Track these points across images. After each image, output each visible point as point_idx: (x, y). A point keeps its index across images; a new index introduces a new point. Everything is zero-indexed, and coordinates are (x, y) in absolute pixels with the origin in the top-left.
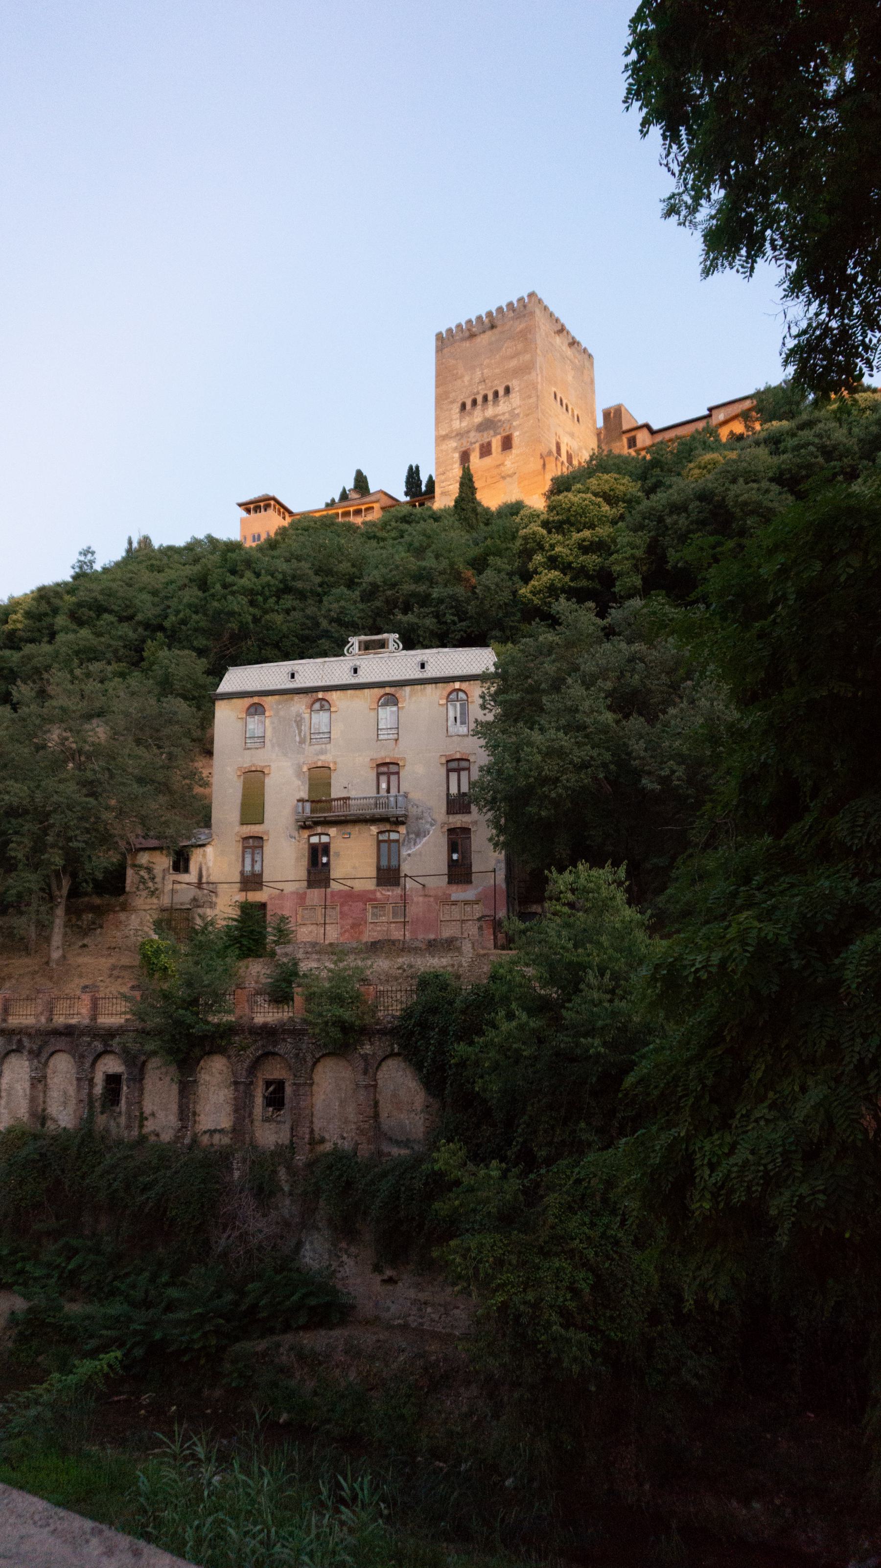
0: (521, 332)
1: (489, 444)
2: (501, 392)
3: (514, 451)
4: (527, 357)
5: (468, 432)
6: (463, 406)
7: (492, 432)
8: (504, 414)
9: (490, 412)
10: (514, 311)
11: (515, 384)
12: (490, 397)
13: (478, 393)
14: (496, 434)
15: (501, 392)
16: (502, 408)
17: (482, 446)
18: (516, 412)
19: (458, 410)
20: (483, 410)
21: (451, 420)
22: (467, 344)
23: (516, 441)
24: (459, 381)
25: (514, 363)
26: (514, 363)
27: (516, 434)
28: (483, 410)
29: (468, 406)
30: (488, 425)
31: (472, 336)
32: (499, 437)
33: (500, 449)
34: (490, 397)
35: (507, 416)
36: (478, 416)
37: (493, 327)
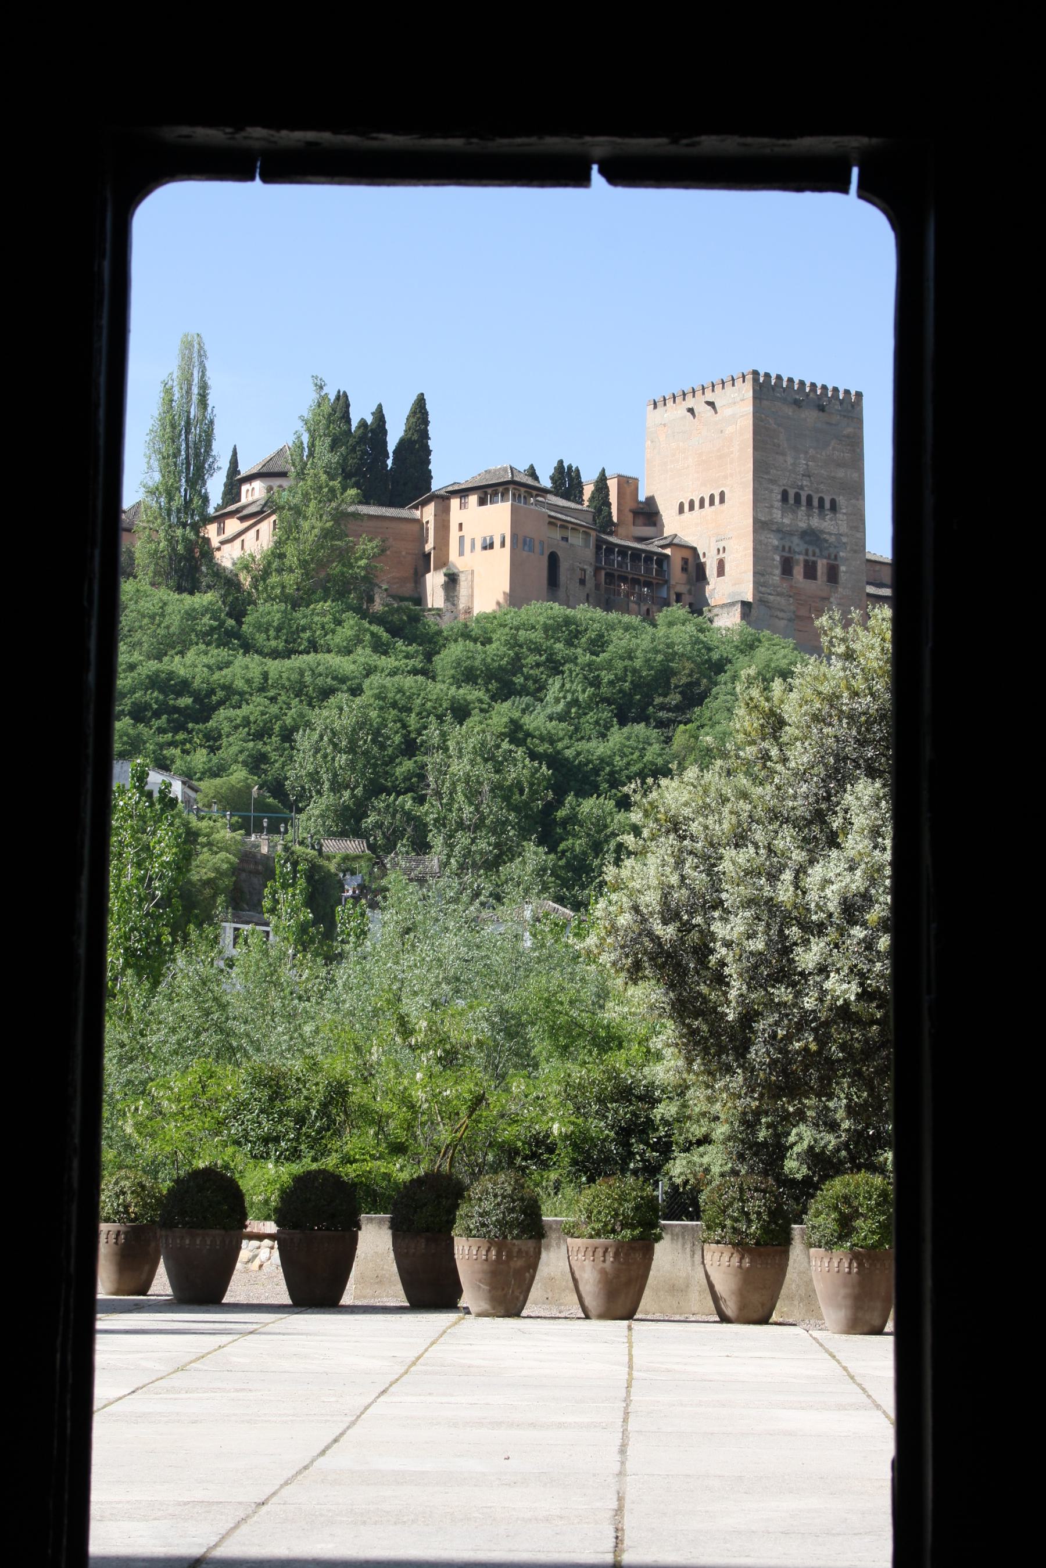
0: (848, 437)
1: (815, 563)
2: (827, 505)
3: (840, 590)
4: (855, 475)
5: (791, 534)
6: (785, 496)
7: (817, 551)
8: (830, 534)
9: (815, 522)
10: (841, 402)
11: (841, 500)
12: (815, 503)
13: (801, 488)
14: (822, 557)
15: (827, 505)
16: (826, 524)
17: (806, 562)
18: (844, 540)
19: (779, 497)
20: (809, 516)
21: (772, 507)
22: (789, 411)
23: (843, 577)
24: (780, 458)
25: (840, 473)
26: (840, 473)
27: (843, 568)
28: (809, 516)
29: (791, 501)
30: (811, 536)
31: (797, 403)
32: (825, 561)
33: (825, 578)
34: (815, 503)
35: (832, 539)
36: (802, 520)
37: (822, 409)
